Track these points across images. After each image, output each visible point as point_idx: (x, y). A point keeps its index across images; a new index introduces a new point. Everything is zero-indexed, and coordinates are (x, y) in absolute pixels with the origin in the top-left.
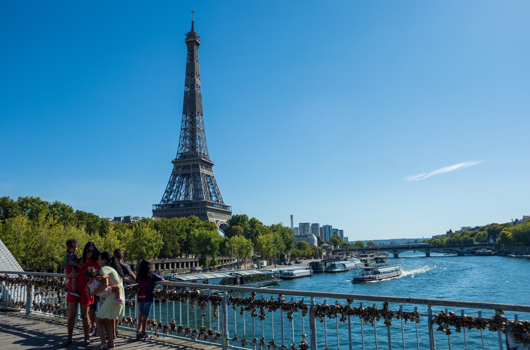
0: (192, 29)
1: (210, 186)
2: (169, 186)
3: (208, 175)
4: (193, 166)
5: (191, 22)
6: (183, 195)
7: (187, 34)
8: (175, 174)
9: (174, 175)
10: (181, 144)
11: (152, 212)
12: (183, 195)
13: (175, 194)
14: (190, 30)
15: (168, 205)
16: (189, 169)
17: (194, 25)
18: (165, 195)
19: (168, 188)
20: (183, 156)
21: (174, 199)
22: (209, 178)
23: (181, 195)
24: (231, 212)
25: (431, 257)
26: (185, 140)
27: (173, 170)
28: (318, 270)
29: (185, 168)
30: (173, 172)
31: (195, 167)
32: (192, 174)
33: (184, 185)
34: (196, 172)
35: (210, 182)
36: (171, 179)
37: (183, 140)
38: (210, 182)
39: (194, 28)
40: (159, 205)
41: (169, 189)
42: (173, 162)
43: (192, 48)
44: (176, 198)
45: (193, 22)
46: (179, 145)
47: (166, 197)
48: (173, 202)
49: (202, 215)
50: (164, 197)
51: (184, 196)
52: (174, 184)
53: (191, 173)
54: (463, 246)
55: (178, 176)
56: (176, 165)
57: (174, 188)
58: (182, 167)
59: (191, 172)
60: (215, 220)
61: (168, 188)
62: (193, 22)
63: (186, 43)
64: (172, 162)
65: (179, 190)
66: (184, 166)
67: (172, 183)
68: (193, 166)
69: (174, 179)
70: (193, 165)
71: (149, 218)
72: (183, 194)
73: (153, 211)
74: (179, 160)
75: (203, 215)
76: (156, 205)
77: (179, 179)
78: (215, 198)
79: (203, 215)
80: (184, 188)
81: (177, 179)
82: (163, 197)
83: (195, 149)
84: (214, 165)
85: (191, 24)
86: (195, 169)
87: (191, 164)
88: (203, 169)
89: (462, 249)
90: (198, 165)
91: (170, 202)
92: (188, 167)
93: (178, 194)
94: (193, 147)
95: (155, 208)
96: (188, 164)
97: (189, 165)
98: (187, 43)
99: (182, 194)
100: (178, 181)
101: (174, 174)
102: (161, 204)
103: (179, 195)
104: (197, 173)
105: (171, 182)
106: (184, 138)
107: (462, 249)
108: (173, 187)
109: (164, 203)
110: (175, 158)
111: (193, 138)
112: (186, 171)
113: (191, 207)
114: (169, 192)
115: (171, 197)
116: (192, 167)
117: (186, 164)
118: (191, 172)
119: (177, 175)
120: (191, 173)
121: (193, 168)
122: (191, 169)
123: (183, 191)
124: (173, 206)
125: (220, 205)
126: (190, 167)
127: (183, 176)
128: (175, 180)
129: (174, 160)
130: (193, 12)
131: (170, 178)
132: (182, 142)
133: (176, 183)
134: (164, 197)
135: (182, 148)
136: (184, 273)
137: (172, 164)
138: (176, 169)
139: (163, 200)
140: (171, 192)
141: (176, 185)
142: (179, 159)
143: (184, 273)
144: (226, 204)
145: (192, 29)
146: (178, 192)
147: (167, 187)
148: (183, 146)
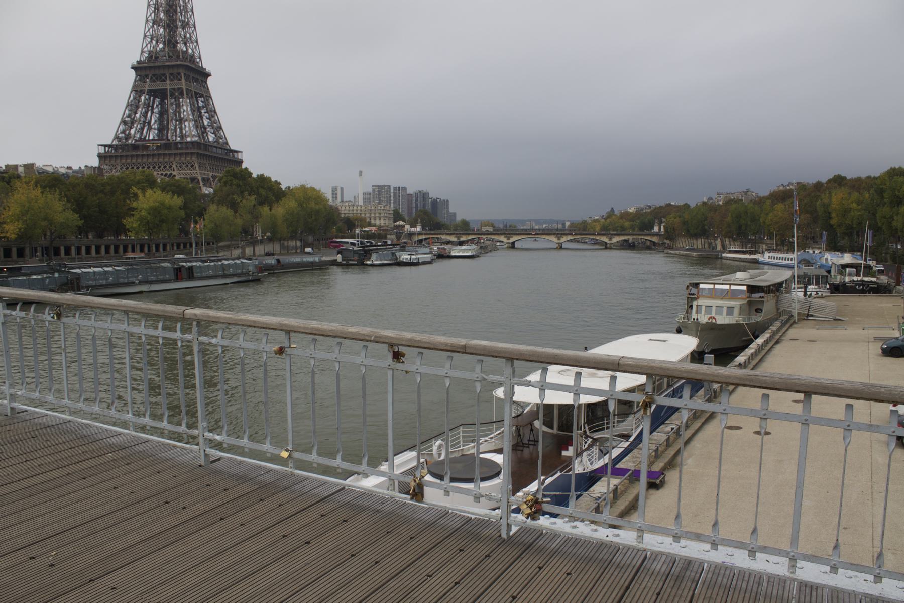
1: (203, 113)
2: (127, 112)
3: (199, 94)
4: (172, 77)
6: (154, 129)
8: (139, 90)
9: (136, 91)
10: (148, 34)
11: (98, 158)
12: (154, 129)
13: (139, 126)
15: (127, 145)
16: (164, 81)
18: (121, 127)
19: (125, 115)
20: (153, 56)
21: (138, 135)
22: (202, 99)
23: (152, 128)
24: (242, 162)
25: (518, 249)
26: (155, 26)
27: (135, 81)
28: (350, 262)
29: (157, 79)
30: (134, 86)
31: (174, 77)
32: (170, 92)
33: (156, 110)
34: (176, 87)
35: (203, 107)
36: (132, 98)
37: (153, 27)
38: (203, 107)
40: (110, 146)
41: (129, 116)
42: (133, 68)
44: (142, 134)
46: (145, 36)
47: (123, 132)
48: (136, 141)
49: (187, 166)
50: (119, 132)
51: (156, 132)
52: (137, 107)
53: (167, 89)
54: (612, 234)
55: (144, 93)
56: (139, 73)
57: (138, 115)
58: (151, 78)
59: (168, 87)
60: (211, 174)
61: (125, 115)
64: (132, 68)
65: (146, 119)
66: (154, 75)
67: (133, 106)
68: (172, 77)
69: (137, 100)
70: (171, 74)
71: (80, 168)
72: (156, 126)
73: (100, 156)
74: (146, 65)
75: (189, 167)
76: (105, 146)
77: (145, 99)
78: (213, 136)
79: (189, 167)
80: (157, 115)
81: (143, 98)
82: (117, 131)
83: (175, 46)
84: (210, 75)
86: (176, 82)
88: (190, 82)
89: (610, 239)
90: (179, 74)
91: (130, 141)
92: (161, 78)
93: (144, 126)
94: (171, 43)
95: (102, 150)
96: (162, 72)
97: (164, 75)
99: (153, 127)
100: (145, 103)
101: (137, 91)
102: (114, 143)
103: (146, 129)
104: (179, 89)
105: (131, 105)
106: (154, 23)
107: (610, 239)
108: (136, 113)
109: (118, 141)
110: (138, 60)
111: (171, 26)
112: (159, 86)
113: (166, 152)
114: (128, 122)
115: (133, 131)
116: (170, 78)
117: (157, 72)
118: (168, 87)
119: (141, 91)
120: (167, 89)
121: (172, 81)
122: (168, 82)
123: (155, 121)
124: (135, 147)
125: (222, 149)
126: (166, 78)
127: (153, 93)
128: (139, 102)
129: (135, 63)
131: (130, 97)
132: (151, 30)
133: (141, 106)
134: (119, 132)
135: (151, 41)
137: (133, 72)
138: (140, 80)
139: (117, 137)
140: (132, 123)
141: (140, 109)
142: (144, 62)
144: (233, 146)
146: (144, 122)
147: (124, 114)
148: (152, 39)
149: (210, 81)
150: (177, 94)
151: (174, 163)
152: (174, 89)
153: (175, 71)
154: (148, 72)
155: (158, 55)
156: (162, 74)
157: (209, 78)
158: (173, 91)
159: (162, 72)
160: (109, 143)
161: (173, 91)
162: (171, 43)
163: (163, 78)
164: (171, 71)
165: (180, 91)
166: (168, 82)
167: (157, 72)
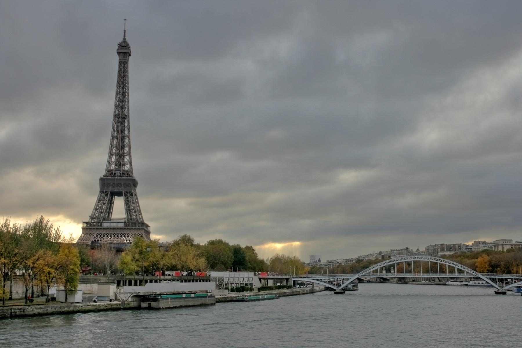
0: (124, 39)
5: (123, 31)
7: (119, 44)
14: (121, 40)
16: (120, 187)
34: (128, 191)
39: (126, 37)
43: (124, 60)
45: (125, 32)
62: (125, 32)
63: (118, 53)
85: (123, 34)
92: (118, 185)
94: (120, 164)
97: (120, 184)
98: (119, 53)
104: (130, 192)
111: (121, 156)
130: (125, 20)
145: (124, 39)
150: (128, 195)
151: (130, 234)
152: (127, 192)
155: (115, 172)
156: (119, 183)
158: (126, 193)
160: (87, 221)
161: (126, 193)
162: (120, 164)
165: (130, 193)
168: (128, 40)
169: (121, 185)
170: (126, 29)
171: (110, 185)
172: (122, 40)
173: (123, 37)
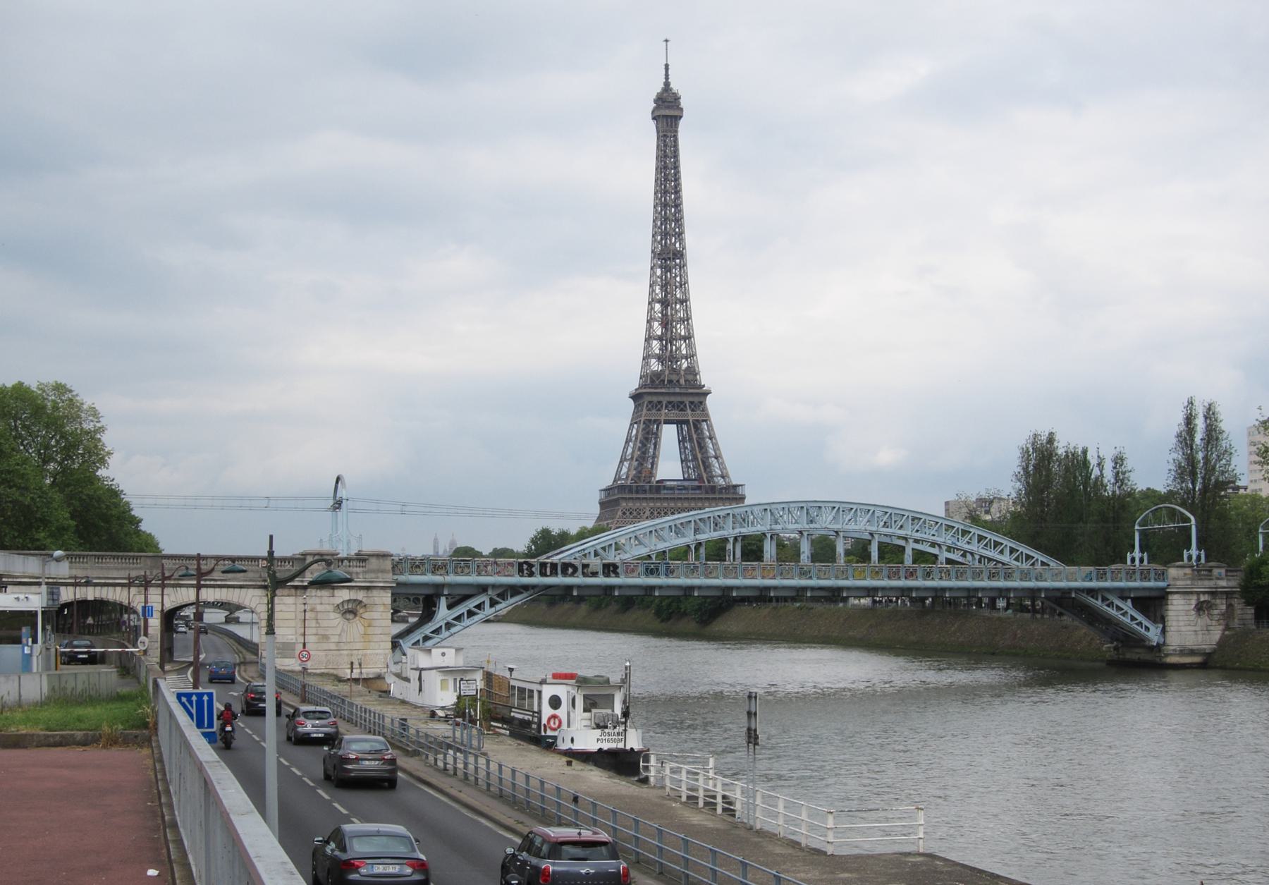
0: (667, 84)
16: (682, 410)
17: (670, 72)
45: (667, 67)
62: (667, 67)
66: (670, 403)
70: (692, 403)
87: (687, 400)
92: (678, 406)
96: (679, 399)
97: (682, 403)
116: (690, 407)
117: (673, 399)
136: (690, 648)
143: (690, 648)
145: (667, 84)
149: (709, 400)
153: (696, 399)
154: (661, 398)
156: (680, 402)
157: (709, 396)
159: (679, 399)
163: (682, 406)
164: (691, 399)
166: (689, 411)
167: (673, 399)
168: (674, 86)
169: (685, 406)
170: (669, 63)
171: (662, 406)
172: (662, 86)
173: (664, 80)
